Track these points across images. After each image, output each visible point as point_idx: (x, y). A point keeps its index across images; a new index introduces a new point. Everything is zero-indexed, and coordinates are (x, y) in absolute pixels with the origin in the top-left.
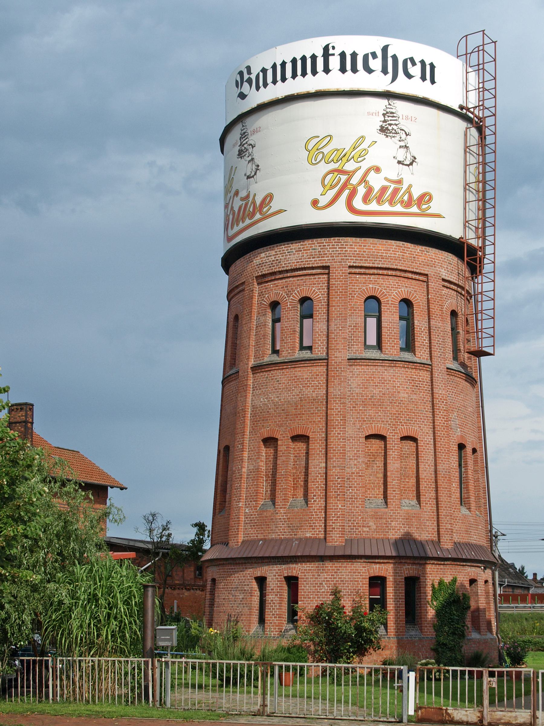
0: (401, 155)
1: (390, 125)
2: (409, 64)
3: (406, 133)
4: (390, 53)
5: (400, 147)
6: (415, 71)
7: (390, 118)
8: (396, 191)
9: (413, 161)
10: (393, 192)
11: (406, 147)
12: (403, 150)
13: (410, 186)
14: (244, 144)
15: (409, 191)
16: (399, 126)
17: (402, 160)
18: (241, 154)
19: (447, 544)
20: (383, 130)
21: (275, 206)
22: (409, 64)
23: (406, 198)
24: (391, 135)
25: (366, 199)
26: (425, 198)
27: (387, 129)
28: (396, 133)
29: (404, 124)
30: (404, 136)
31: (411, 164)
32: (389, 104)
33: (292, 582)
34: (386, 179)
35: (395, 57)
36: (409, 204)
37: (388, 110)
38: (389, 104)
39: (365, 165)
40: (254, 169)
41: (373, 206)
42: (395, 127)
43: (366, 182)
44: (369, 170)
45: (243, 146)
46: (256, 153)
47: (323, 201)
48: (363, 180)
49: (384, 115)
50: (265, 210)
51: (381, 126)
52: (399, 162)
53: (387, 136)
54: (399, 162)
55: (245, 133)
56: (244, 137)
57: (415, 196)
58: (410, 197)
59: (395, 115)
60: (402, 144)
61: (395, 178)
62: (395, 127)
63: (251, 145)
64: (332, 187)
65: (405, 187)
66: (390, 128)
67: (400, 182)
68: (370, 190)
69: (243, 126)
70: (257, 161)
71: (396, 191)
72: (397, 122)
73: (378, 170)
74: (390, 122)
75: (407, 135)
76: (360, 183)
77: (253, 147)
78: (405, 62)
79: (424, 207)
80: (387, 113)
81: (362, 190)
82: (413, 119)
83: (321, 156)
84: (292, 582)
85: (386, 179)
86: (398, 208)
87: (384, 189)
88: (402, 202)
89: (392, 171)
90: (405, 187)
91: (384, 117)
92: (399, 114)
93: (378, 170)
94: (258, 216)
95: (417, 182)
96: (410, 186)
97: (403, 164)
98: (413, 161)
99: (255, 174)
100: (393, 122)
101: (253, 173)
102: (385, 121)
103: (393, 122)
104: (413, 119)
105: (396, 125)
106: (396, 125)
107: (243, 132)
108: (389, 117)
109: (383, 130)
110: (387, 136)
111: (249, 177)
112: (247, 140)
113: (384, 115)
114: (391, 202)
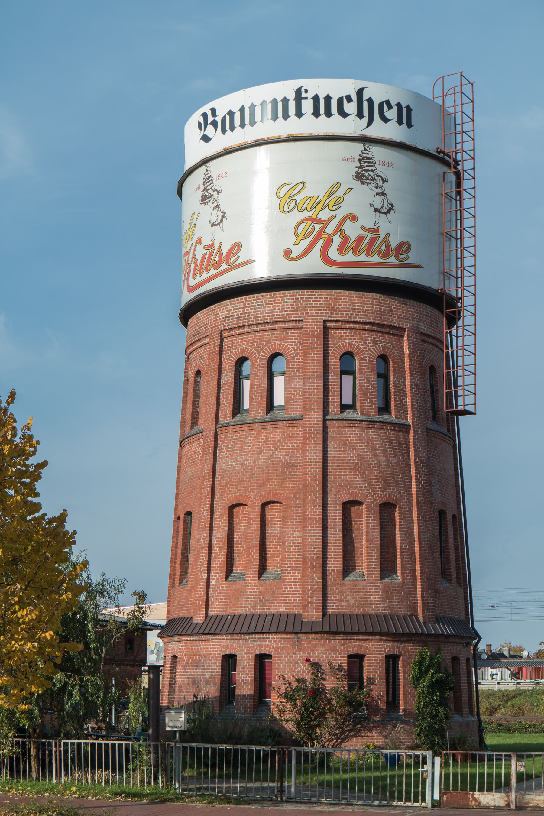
0: (378, 202)
1: (367, 171)
2: (385, 108)
3: (382, 179)
6: (391, 114)
7: (366, 164)
8: (373, 241)
9: (391, 209)
11: (383, 194)
12: (379, 198)
14: (209, 189)
15: (386, 240)
17: (379, 207)
18: (204, 199)
20: (359, 176)
21: (243, 256)
22: (385, 108)
23: (383, 248)
24: (367, 181)
25: (341, 250)
27: (363, 175)
28: (373, 180)
30: (380, 183)
31: (389, 212)
34: (362, 228)
35: (370, 101)
36: (386, 255)
37: (364, 156)
38: (365, 150)
39: (340, 214)
40: (220, 217)
41: (350, 257)
42: (372, 174)
45: (207, 191)
46: (222, 199)
47: (296, 251)
48: (339, 229)
50: (232, 260)
52: (376, 210)
53: (363, 183)
54: (376, 210)
55: (209, 178)
56: (208, 182)
59: (371, 160)
60: (379, 190)
61: (371, 226)
62: (372, 174)
63: (216, 190)
64: (305, 237)
65: (382, 236)
66: (366, 174)
67: (377, 231)
68: (346, 239)
69: (207, 170)
70: (223, 208)
72: (374, 168)
73: (354, 218)
74: (366, 168)
75: (384, 181)
76: (335, 233)
77: (218, 193)
78: (381, 105)
79: (402, 257)
80: (363, 158)
81: (337, 240)
82: (390, 164)
83: (293, 203)
85: (362, 228)
86: (376, 259)
87: (360, 239)
88: (379, 252)
91: (360, 163)
92: (376, 159)
93: (354, 218)
94: (224, 266)
96: (388, 235)
97: (380, 212)
98: (391, 209)
99: (221, 221)
100: (369, 168)
101: (219, 221)
102: (360, 167)
103: (369, 168)
105: (372, 171)
106: (372, 171)
107: (207, 176)
108: (365, 162)
109: (359, 176)
111: (213, 225)
112: (211, 185)
113: (360, 160)
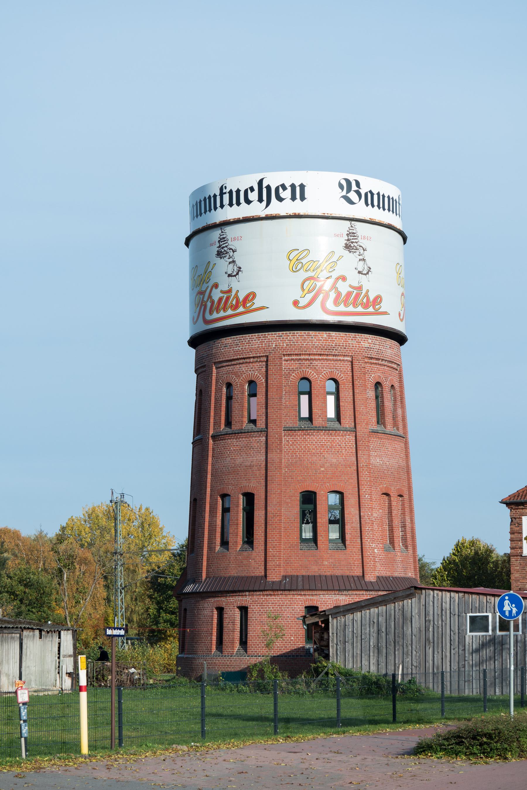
0: (361, 266)
1: (352, 242)
2: (281, 190)
3: (363, 249)
4: (265, 184)
5: (360, 260)
6: (286, 194)
7: (352, 238)
8: (358, 295)
9: (369, 271)
10: (356, 296)
11: (364, 260)
12: (362, 263)
13: (368, 291)
14: (224, 247)
15: (367, 295)
16: (359, 243)
17: (361, 270)
18: (220, 254)
19: (370, 577)
20: (347, 247)
21: (258, 303)
22: (281, 190)
23: (365, 301)
24: (353, 250)
25: (336, 302)
26: (378, 300)
27: (350, 246)
28: (357, 249)
29: (362, 242)
30: (362, 251)
31: (368, 273)
32: (352, 227)
33: (244, 610)
34: (351, 286)
35: (268, 188)
36: (366, 306)
37: (351, 231)
38: (352, 227)
39: (335, 275)
40: (236, 270)
41: (342, 308)
42: (356, 244)
43: (336, 289)
44: (338, 279)
45: (223, 248)
46: (237, 257)
47: (302, 303)
48: (334, 287)
49: (347, 235)
50: (248, 305)
51: (346, 244)
52: (359, 272)
53: (350, 252)
54: (359, 272)
55: (224, 238)
56: (224, 241)
57: (371, 299)
58: (368, 300)
59: (355, 235)
60: (361, 257)
61: (356, 285)
62: (356, 244)
63: (231, 249)
64: (309, 292)
65: (364, 292)
66: (352, 245)
67: (360, 288)
68: (339, 294)
69: (222, 232)
70: (239, 263)
71: (358, 295)
72: (357, 241)
73: (344, 279)
74: (352, 241)
75: (364, 250)
76: (331, 290)
77: (234, 252)
78: (277, 189)
79: (377, 307)
80: (350, 233)
81: (333, 295)
82: (369, 238)
83: (300, 265)
84: (244, 610)
85: (351, 286)
86: (360, 309)
87: (349, 294)
88: (362, 304)
89: (354, 279)
90: (364, 292)
91: (348, 237)
92: (359, 234)
93: (344, 279)
94: (241, 309)
95: (372, 286)
96: (368, 291)
97: (362, 274)
98: (369, 271)
99: (237, 274)
100: (354, 241)
101: (235, 273)
102: (348, 240)
103: (354, 241)
104: (369, 238)
105: (356, 243)
106: (356, 243)
107: (222, 237)
108: (351, 236)
109: (347, 247)
110: (350, 252)
111: (229, 276)
112: (227, 244)
113: (347, 235)
114: (355, 305)
